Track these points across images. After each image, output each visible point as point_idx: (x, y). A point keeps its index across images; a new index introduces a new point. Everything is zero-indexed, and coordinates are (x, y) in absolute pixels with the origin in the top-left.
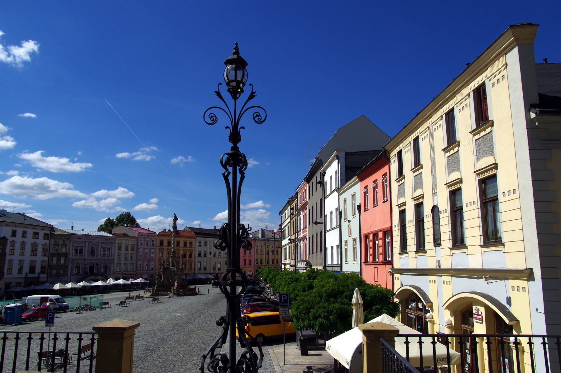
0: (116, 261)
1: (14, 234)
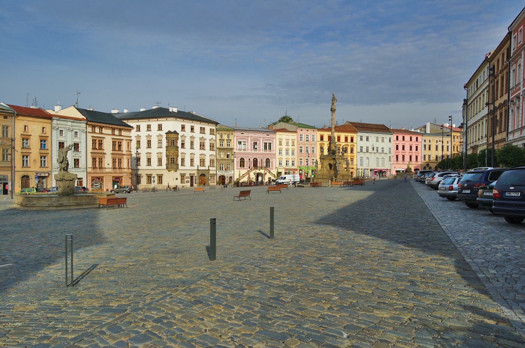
0: (278, 156)
1: (183, 128)
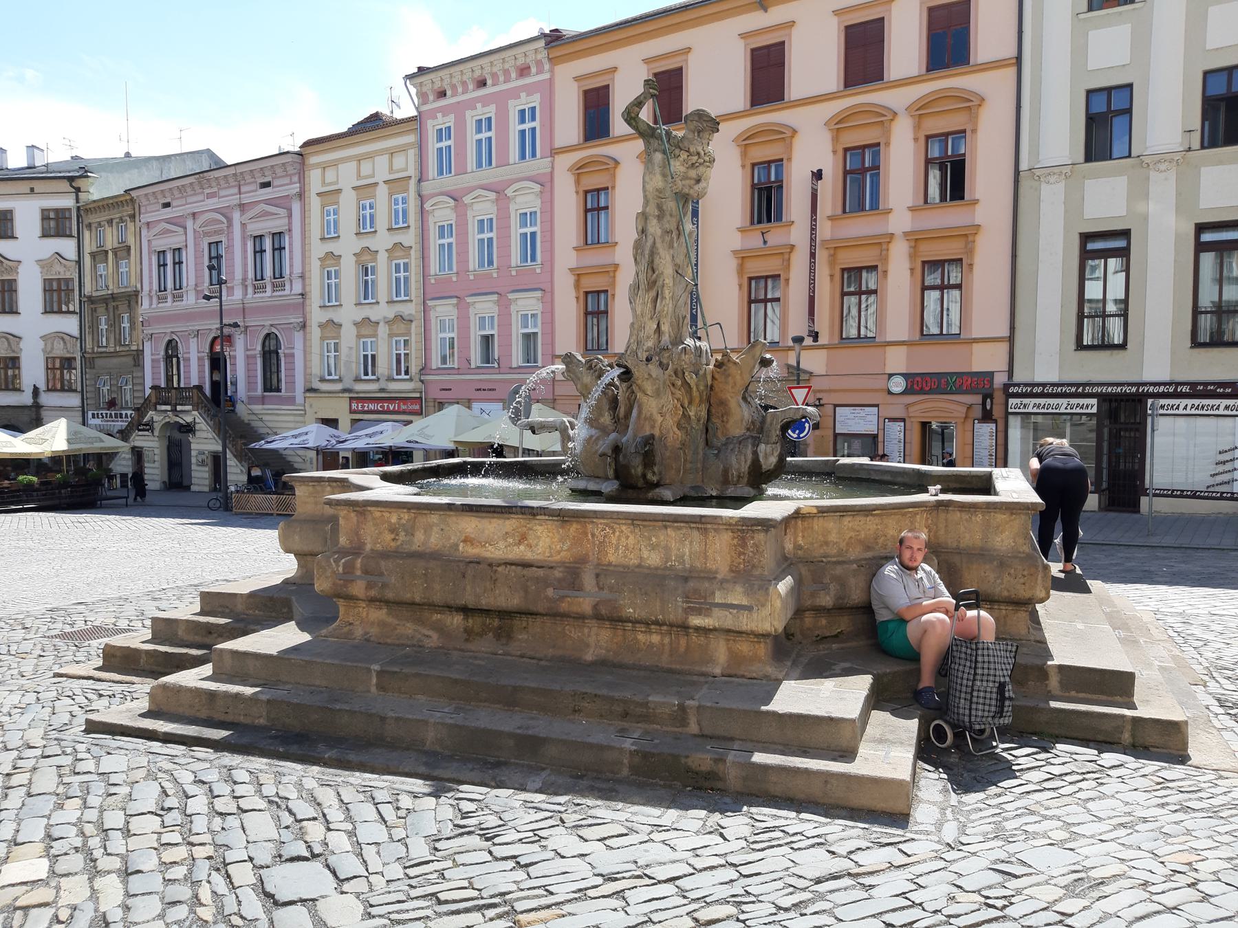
0: (317, 316)
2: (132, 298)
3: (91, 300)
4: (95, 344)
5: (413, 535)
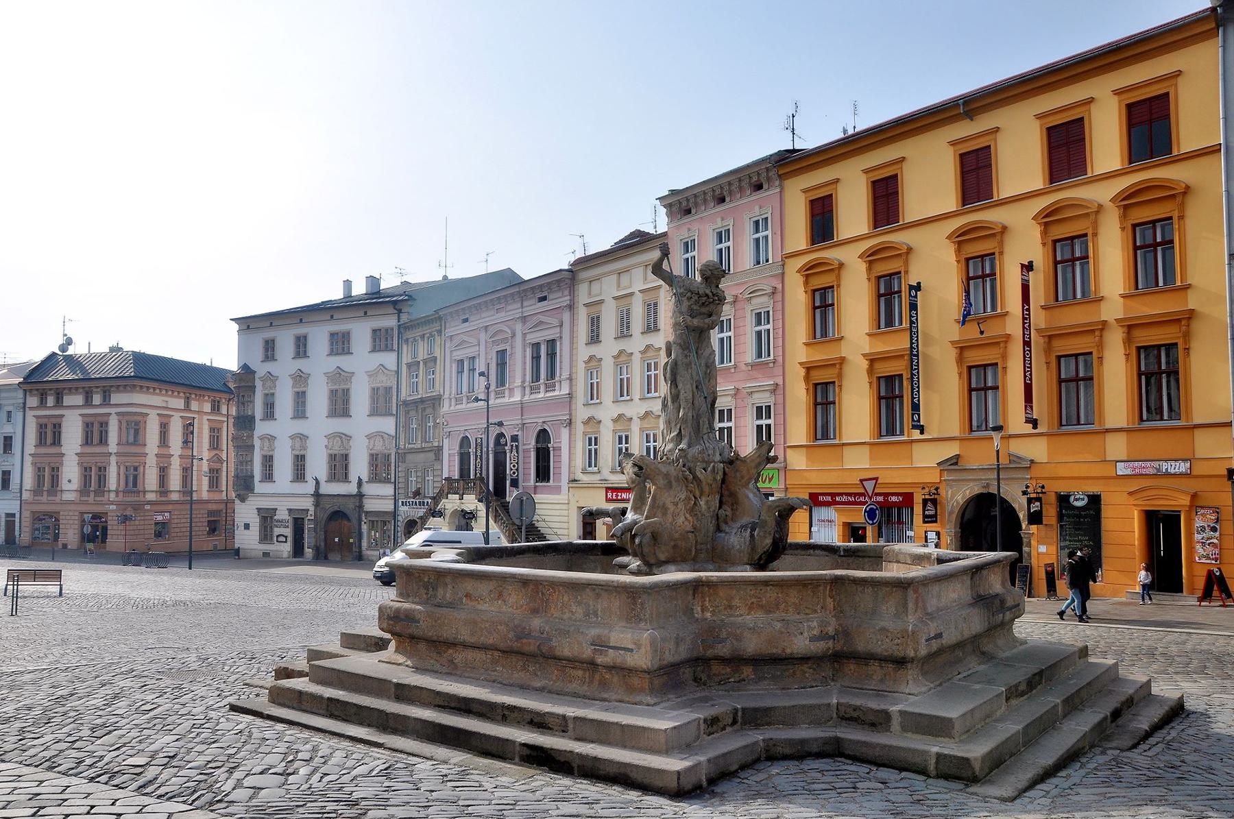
0: (581, 413)
2: (436, 401)
3: (405, 403)
4: (407, 441)
5: (436, 590)
